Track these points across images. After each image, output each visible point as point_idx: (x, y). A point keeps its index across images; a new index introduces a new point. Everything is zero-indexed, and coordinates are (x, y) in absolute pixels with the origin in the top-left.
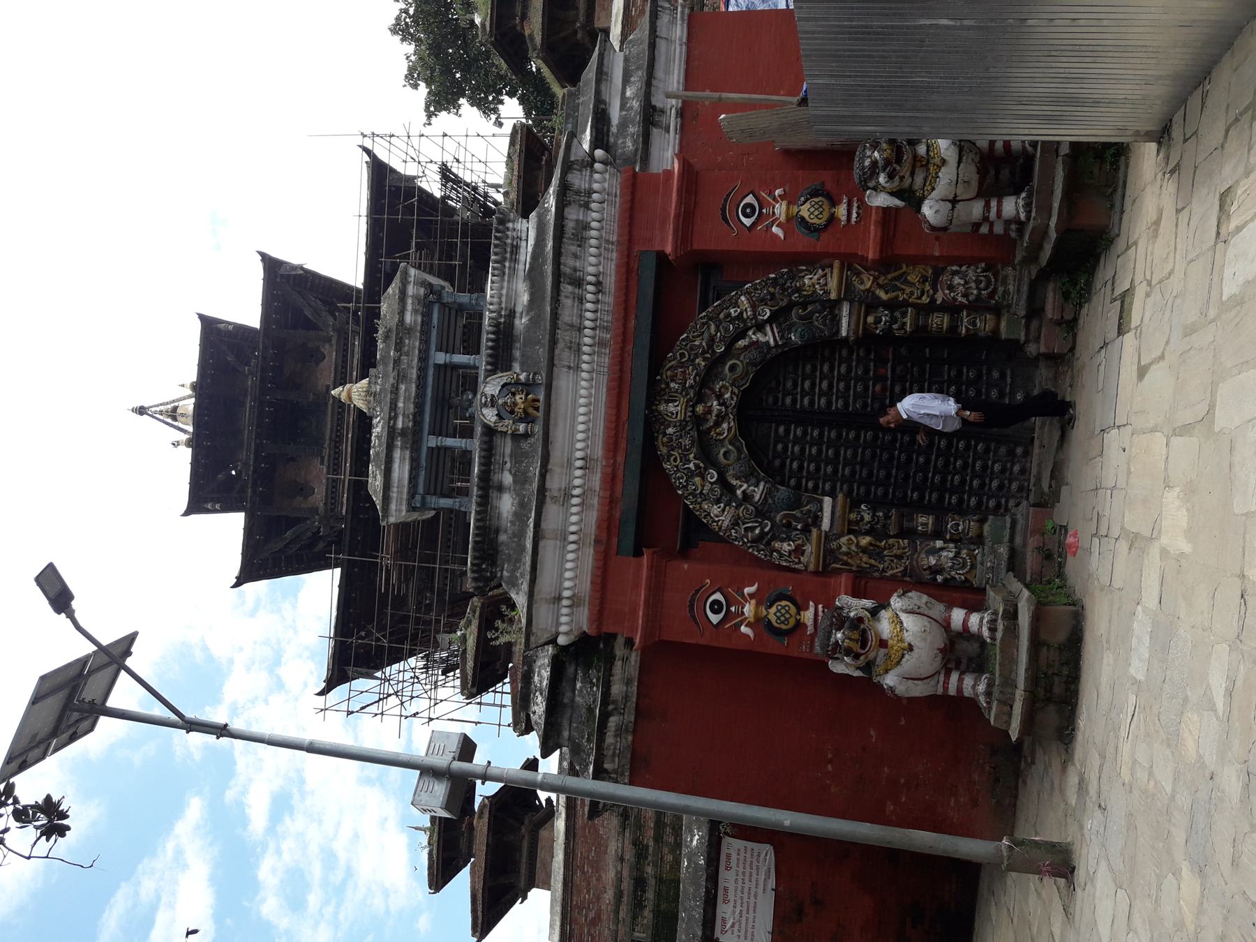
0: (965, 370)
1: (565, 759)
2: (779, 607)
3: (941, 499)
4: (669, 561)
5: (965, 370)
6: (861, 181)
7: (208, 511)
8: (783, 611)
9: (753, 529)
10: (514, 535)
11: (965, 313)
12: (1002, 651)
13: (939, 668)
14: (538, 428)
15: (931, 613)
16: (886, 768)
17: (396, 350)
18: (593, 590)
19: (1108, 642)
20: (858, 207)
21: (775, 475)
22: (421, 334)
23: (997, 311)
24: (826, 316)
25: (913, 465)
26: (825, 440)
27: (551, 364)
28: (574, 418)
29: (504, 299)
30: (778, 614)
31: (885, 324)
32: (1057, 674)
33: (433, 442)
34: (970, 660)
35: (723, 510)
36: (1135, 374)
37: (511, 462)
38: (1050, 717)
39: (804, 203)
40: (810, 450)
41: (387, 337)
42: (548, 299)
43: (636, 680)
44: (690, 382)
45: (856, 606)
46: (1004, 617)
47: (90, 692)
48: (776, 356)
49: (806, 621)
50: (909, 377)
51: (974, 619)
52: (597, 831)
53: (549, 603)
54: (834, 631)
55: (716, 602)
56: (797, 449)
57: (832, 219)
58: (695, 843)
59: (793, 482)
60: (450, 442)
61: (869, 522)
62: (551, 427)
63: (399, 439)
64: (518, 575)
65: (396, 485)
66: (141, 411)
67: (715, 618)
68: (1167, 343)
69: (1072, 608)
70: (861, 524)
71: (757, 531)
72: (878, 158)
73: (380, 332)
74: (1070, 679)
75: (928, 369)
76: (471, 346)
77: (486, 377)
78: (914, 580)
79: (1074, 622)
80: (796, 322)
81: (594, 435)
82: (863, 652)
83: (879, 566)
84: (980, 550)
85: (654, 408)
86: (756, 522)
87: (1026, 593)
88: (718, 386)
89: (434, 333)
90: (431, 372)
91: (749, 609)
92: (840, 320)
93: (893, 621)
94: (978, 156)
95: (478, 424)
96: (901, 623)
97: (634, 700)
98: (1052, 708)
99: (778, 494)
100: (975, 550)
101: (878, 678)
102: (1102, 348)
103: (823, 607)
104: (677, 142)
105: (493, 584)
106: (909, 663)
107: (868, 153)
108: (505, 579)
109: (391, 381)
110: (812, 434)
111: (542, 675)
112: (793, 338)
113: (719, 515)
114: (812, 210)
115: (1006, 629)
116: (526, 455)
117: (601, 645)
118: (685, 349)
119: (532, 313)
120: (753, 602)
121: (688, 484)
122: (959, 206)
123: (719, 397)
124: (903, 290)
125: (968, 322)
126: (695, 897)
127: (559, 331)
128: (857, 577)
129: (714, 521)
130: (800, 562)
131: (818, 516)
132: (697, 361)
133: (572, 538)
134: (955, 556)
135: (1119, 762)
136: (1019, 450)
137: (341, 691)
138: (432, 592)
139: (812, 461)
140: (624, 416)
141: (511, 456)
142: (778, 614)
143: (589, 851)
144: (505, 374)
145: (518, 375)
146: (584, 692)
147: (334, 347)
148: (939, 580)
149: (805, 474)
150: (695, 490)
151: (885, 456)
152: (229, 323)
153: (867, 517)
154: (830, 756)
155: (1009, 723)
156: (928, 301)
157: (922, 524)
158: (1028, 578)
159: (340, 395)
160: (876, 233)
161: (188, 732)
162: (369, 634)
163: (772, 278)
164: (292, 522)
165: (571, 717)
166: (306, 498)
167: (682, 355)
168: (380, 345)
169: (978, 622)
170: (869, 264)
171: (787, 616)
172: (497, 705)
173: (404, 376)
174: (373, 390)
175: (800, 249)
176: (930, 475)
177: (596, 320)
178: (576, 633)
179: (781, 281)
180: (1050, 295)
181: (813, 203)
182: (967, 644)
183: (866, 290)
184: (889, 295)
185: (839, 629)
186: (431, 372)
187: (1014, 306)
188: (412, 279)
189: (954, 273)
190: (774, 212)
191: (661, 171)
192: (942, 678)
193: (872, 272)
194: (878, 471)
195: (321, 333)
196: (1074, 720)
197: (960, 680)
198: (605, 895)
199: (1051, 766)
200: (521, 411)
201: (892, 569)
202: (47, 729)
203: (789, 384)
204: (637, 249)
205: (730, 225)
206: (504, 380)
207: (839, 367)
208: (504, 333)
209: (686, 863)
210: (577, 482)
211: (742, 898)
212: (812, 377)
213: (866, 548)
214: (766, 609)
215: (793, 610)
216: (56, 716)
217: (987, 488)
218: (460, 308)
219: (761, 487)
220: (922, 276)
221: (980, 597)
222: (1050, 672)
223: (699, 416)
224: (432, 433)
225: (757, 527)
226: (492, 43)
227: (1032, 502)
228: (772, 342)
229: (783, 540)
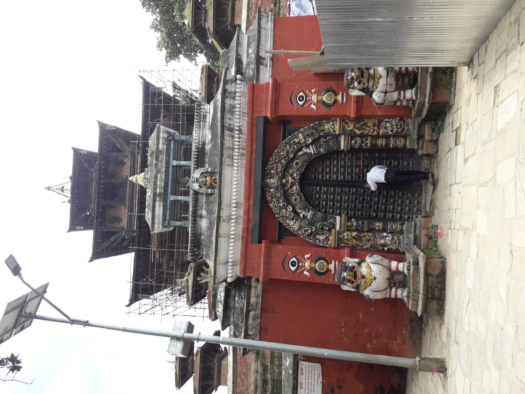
0: (393, 162)
1: (232, 330)
2: (320, 263)
4: (273, 245)
5: (393, 162)
6: (347, 85)
7: (78, 230)
8: (321, 265)
9: (308, 230)
10: (208, 236)
11: (392, 138)
12: (413, 278)
13: (387, 287)
14: (216, 191)
15: (383, 263)
16: (366, 330)
17: (156, 160)
18: (241, 258)
19: (457, 273)
20: (346, 96)
21: (316, 207)
22: (166, 153)
23: (405, 137)
24: (335, 141)
25: (373, 202)
26: (336, 192)
27: (221, 164)
28: (231, 186)
29: (200, 138)
30: (319, 266)
31: (359, 144)
32: (436, 287)
33: (172, 198)
34: (400, 282)
35: (295, 223)
36: (463, 161)
37: (205, 205)
38: (434, 305)
39: (324, 95)
40: (330, 197)
41: (152, 155)
42: (219, 137)
43: (261, 296)
44: (279, 170)
45: (351, 262)
46: (413, 264)
47: (29, 309)
49: (331, 268)
50: (370, 165)
51: (401, 265)
52: (246, 360)
53: (223, 265)
54: (343, 272)
55: (293, 262)
56: (325, 196)
57: (336, 101)
58: (287, 364)
59: (323, 210)
60: (179, 198)
61: (356, 226)
62: (222, 190)
63: (158, 197)
64: (210, 253)
65: (157, 217)
66: (49, 189)
67: (293, 269)
68: (476, 148)
69: (441, 259)
70: (352, 227)
71: (309, 231)
72: (354, 76)
73: (149, 152)
74: (441, 289)
75: (377, 162)
76: (188, 158)
77: (194, 170)
78: (375, 250)
79: (442, 265)
81: (240, 193)
82: (355, 281)
83: (361, 244)
84: (402, 236)
85: (265, 181)
87: (422, 254)
88: (291, 171)
89: (172, 152)
90: (171, 169)
91: (307, 264)
92: (340, 142)
93: (367, 267)
94: (395, 73)
95: (191, 190)
96: (371, 268)
97: (260, 304)
98: (434, 302)
100: (400, 236)
101: (362, 292)
102: (449, 151)
104: (271, 71)
105: (199, 257)
106: (375, 285)
107: (350, 74)
108: (204, 255)
109: (154, 173)
110: (331, 190)
111: (221, 295)
112: (321, 150)
113: (294, 225)
114: (327, 97)
115: (414, 269)
116: (211, 202)
117: (246, 282)
118: (277, 156)
119: (213, 143)
120: (309, 261)
121: (280, 212)
122: (388, 94)
123: (292, 176)
124: (366, 129)
126: (288, 387)
127: (224, 150)
129: (291, 228)
130: (327, 244)
131: (335, 224)
132: (282, 161)
133: (232, 237)
134: (392, 239)
135: (463, 323)
136: (416, 195)
137: (136, 304)
138: (173, 261)
139: (331, 201)
140: (252, 185)
141: (205, 203)
142: (319, 266)
143: (243, 369)
144: (202, 169)
145: (207, 169)
146: (239, 302)
147: (130, 159)
148: (386, 250)
149: (328, 207)
150: (283, 215)
151: (361, 198)
152: (85, 151)
153: (355, 224)
154: (343, 325)
155: (417, 309)
158: (422, 248)
159: (132, 179)
161: (72, 324)
162: (147, 280)
163: (312, 126)
164: (113, 233)
165: (234, 313)
166: (119, 223)
167: (276, 159)
168: (149, 158)
169: (402, 267)
170: (351, 119)
171: (323, 266)
172: (202, 308)
173: (159, 171)
174: (146, 177)
175: (323, 114)
176: (380, 206)
177: (239, 145)
178: (235, 277)
179: (316, 127)
180: (427, 130)
181: (327, 95)
182: (398, 276)
183: (351, 130)
185: (345, 271)
186: (171, 169)
187: (412, 135)
188: (162, 130)
189: (387, 122)
190: (311, 99)
191: (264, 83)
192: (388, 290)
193: (353, 123)
194: (358, 205)
195: (124, 154)
196: (444, 306)
197: (396, 291)
198: (250, 387)
199: (435, 326)
200: (209, 184)
201: (366, 245)
202: (11, 325)
203: (320, 170)
204: (255, 115)
205: (294, 105)
206: (202, 171)
207: (341, 162)
208: (201, 152)
209: (284, 373)
210: (234, 213)
211: (308, 387)
212: (330, 166)
213: (355, 237)
214: (314, 264)
215: (326, 264)
216: (15, 319)
217: (404, 210)
218: (182, 142)
220: (373, 124)
221: (403, 256)
222: (433, 287)
224: (172, 194)
225: (309, 229)
226: (192, 32)
227: (423, 216)
228: (313, 153)
229: (320, 235)
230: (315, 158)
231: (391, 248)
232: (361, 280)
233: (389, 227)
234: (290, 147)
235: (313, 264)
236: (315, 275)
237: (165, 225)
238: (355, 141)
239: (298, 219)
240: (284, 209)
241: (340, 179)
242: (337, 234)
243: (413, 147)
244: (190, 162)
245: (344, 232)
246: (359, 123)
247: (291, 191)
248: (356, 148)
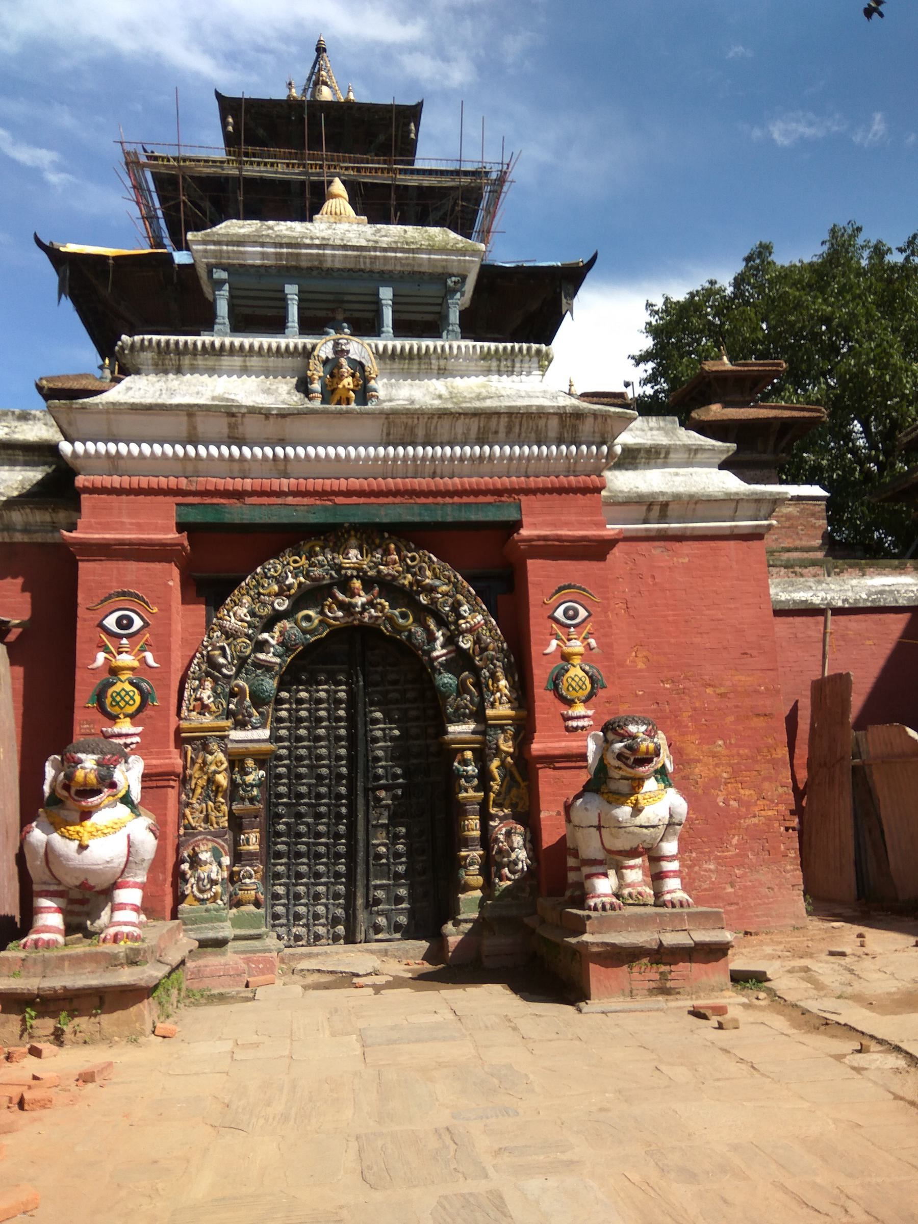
3: (278, 855)
8: (127, 698)
9: (225, 656)
11: (481, 852)
14: (317, 404)
30: (123, 693)
35: (242, 621)
39: (583, 670)
49: (118, 725)
55: (131, 622)
57: (570, 703)
61: (244, 782)
67: (110, 622)
71: (222, 660)
85: (353, 533)
86: (233, 658)
91: (126, 660)
99: (268, 680)
100: (222, 900)
103: (137, 743)
114: (577, 679)
120: (136, 664)
121: (268, 578)
123: (371, 604)
128: (178, 776)
129: (228, 611)
130: (189, 711)
132: (409, 576)
150: (263, 586)
152: (416, 135)
153: (250, 779)
157: (248, 840)
160: (556, 748)
175: (536, 671)
181: (583, 679)
190: (569, 640)
203: (392, 677)
204: (523, 498)
215: (130, 710)
219: (278, 660)
228: (435, 654)
229: (214, 690)
231: (186, 881)
232: (76, 811)
233: (248, 868)
235: (126, 677)
237: (214, 270)
239: (255, 627)
240: (280, 588)
241: (371, 731)
243: (462, 910)
244: (391, 335)
245: (225, 752)
248: (452, 765)
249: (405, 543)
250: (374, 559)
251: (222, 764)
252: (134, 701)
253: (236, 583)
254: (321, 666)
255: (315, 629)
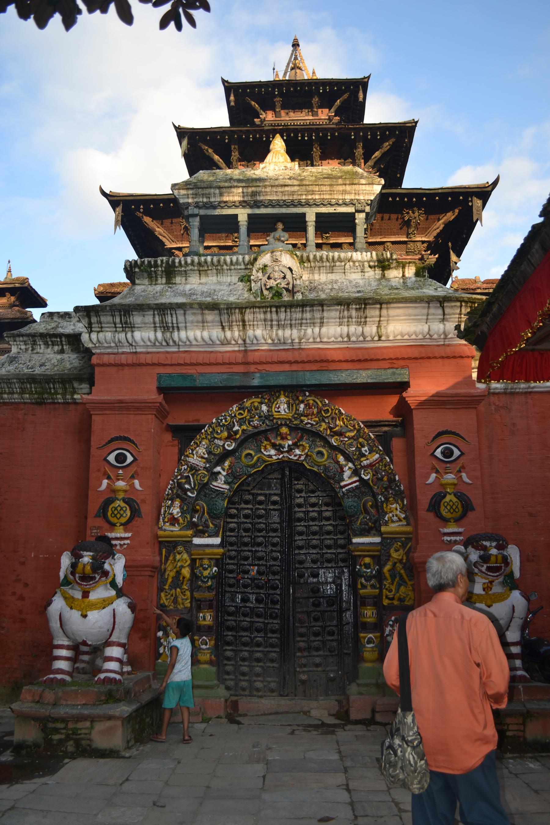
8: (122, 512)
11: (378, 634)
24: (367, 524)
30: (119, 509)
31: (365, 572)
35: (202, 457)
48: (334, 488)
55: (125, 458)
70: (201, 569)
71: (187, 486)
80: (361, 501)
82: (77, 579)
85: (282, 392)
88: (304, 443)
91: (121, 484)
92: (367, 536)
114: (451, 504)
118: (332, 413)
120: (128, 488)
121: (221, 426)
123: (296, 445)
124: (393, 584)
125: (371, 638)
128: (156, 568)
129: (192, 450)
131: (204, 534)
132: (323, 424)
142: (119, 509)
150: (217, 432)
153: (206, 573)
156: (385, 604)
163: (395, 478)
167: (327, 411)
169: (111, 668)
170: (411, 554)
171: (118, 516)
175: (419, 497)
181: (456, 504)
184: (388, 573)
190: (447, 473)
192: (66, 643)
193: (405, 558)
203: (313, 500)
213: (181, 574)
215: (123, 520)
217: (242, 663)
219: (227, 487)
223: (278, 430)
225: (190, 485)
228: (342, 484)
230: (333, 490)
233: (204, 637)
234: (352, 438)
236: (101, 500)
238: (369, 564)
239: (211, 462)
240: (229, 433)
242: (184, 539)
246: (405, 570)
247: (265, 446)
248: (356, 568)
249: (321, 400)
250: (297, 412)
251: (186, 561)
252: (127, 515)
253: (198, 429)
254: (259, 492)
255: (255, 464)
